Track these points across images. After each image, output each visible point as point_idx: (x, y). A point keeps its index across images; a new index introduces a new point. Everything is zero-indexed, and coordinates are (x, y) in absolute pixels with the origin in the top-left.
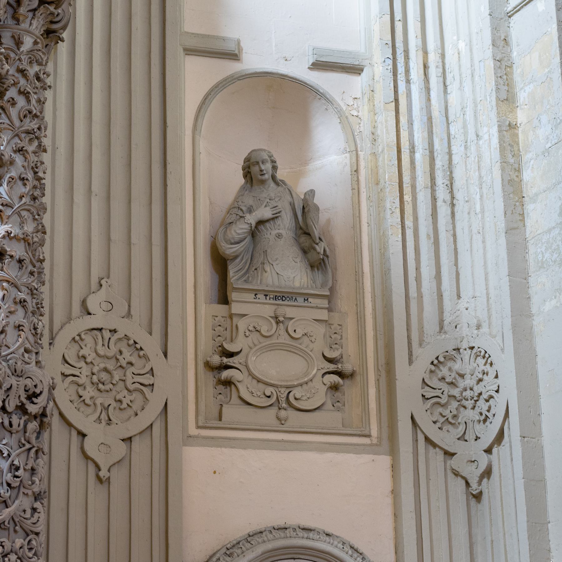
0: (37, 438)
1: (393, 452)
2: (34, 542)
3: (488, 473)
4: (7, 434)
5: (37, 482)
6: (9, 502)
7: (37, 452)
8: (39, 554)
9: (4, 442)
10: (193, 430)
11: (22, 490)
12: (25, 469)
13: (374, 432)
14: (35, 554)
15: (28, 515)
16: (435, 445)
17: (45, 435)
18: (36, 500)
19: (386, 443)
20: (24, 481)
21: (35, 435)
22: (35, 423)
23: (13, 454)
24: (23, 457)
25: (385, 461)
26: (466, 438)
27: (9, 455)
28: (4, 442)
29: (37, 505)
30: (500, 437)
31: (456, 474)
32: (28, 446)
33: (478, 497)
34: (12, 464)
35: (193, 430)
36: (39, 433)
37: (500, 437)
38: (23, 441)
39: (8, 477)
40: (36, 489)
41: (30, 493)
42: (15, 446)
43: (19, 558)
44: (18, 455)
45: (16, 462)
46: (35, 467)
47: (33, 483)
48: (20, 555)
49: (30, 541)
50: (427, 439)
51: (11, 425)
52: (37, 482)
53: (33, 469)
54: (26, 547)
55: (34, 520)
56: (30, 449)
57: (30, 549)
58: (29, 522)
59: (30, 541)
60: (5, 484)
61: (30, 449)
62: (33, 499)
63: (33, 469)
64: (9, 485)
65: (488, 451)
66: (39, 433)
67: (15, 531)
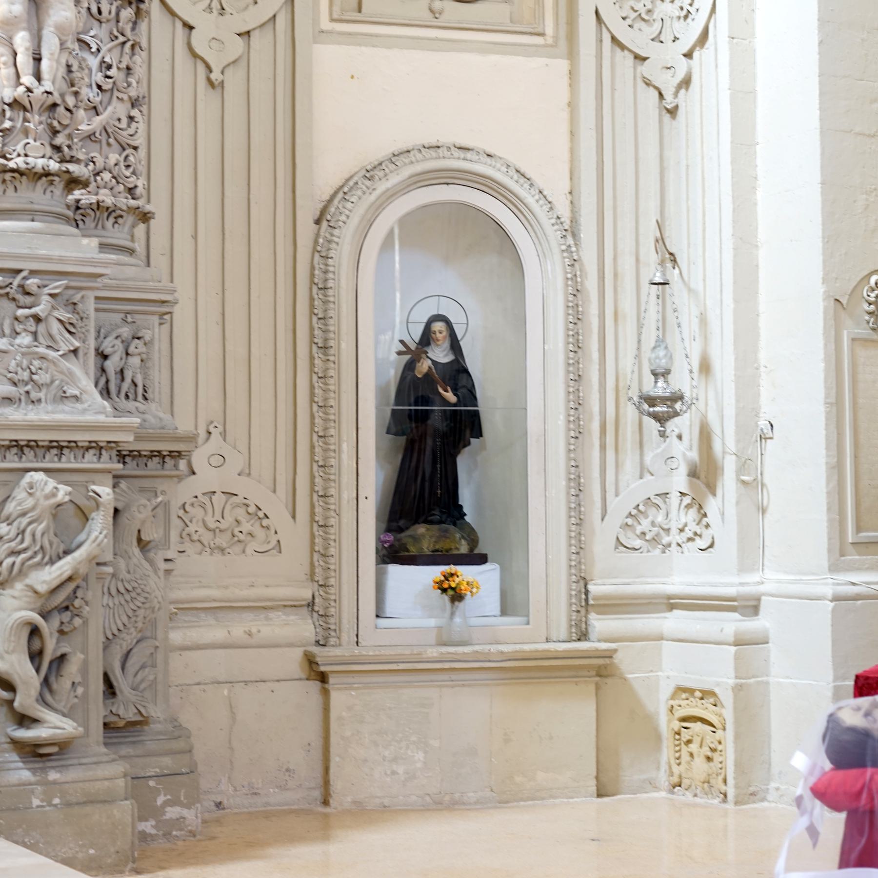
0: (133, 29)
1: (572, 54)
2: (131, 158)
3: (686, 82)
4: (96, 23)
5: (134, 84)
6: (100, 109)
7: (133, 46)
8: (138, 172)
9: (92, 33)
10: (325, 24)
11: (116, 93)
12: (118, 68)
13: (549, 30)
14: (134, 173)
15: (124, 125)
16: (623, 47)
17: (143, 26)
18: (133, 106)
19: (563, 44)
20: (118, 83)
21: (130, 25)
22: (129, 10)
23: (104, 49)
24: (117, 51)
25: (563, 65)
26: (662, 39)
27: (99, 50)
28: (92, 33)
29: (135, 113)
30: (704, 35)
31: (648, 83)
32: (122, 39)
33: (673, 112)
34: (103, 62)
35: (325, 24)
36: (135, 23)
37: (704, 35)
38: (116, 33)
39: (99, 77)
40: (133, 93)
41: (125, 97)
42: (106, 39)
43: (114, 177)
44: (110, 50)
45: (107, 59)
46: (131, 65)
47: (129, 85)
48: (115, 174)
49: (127, 157)
50: (614, 39)
51: (100, 12)
52: (134, 84)
53: (128, 68)
54: (122, 164)
55: (131, 131)
56: (124, 43)
57: (128, 166)
58: (125, 133)
59: (127, 157)
60: (94, 86)
61: (124, 43)
62: (130, 105)
63: (128, 68)
64: (99, 87)
65: (688, 55)
66: (135, 23)
67: (109, 144)
